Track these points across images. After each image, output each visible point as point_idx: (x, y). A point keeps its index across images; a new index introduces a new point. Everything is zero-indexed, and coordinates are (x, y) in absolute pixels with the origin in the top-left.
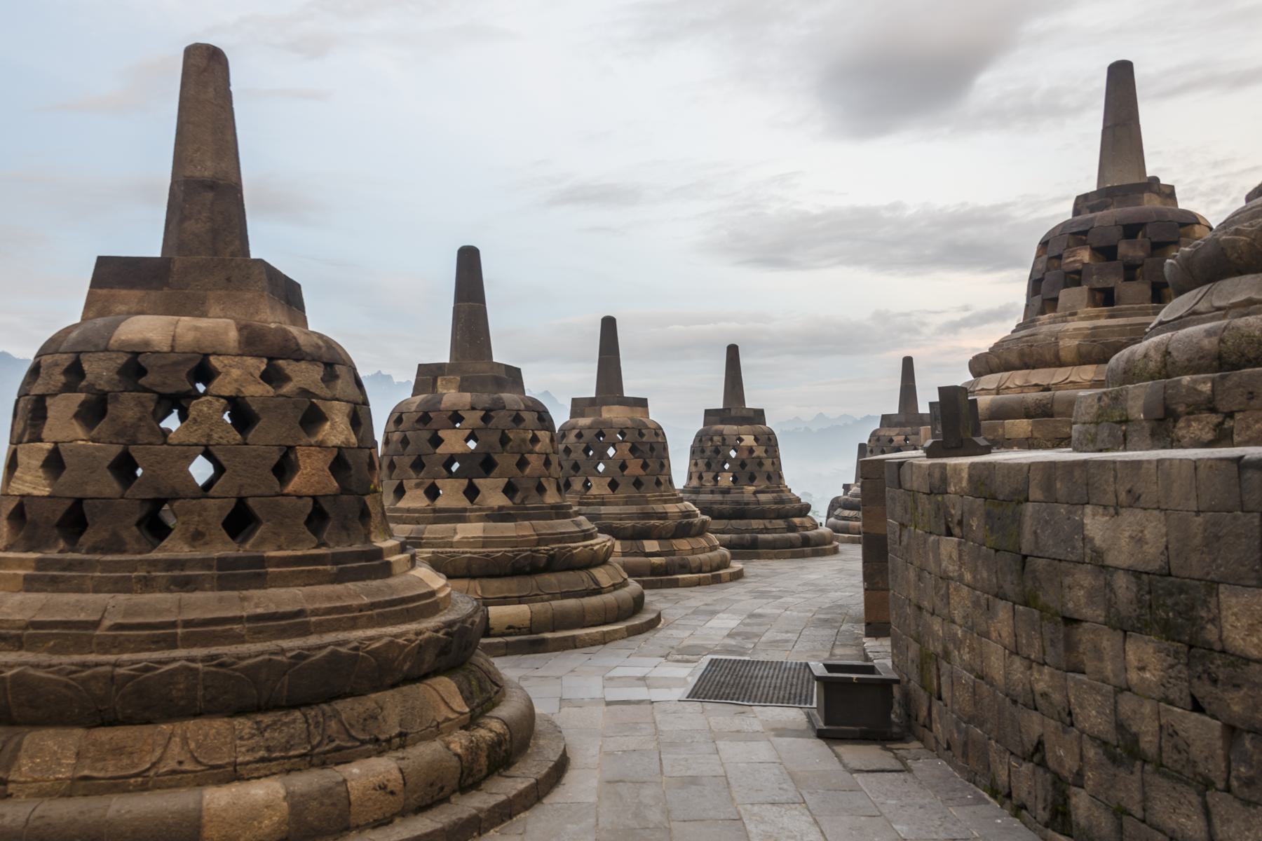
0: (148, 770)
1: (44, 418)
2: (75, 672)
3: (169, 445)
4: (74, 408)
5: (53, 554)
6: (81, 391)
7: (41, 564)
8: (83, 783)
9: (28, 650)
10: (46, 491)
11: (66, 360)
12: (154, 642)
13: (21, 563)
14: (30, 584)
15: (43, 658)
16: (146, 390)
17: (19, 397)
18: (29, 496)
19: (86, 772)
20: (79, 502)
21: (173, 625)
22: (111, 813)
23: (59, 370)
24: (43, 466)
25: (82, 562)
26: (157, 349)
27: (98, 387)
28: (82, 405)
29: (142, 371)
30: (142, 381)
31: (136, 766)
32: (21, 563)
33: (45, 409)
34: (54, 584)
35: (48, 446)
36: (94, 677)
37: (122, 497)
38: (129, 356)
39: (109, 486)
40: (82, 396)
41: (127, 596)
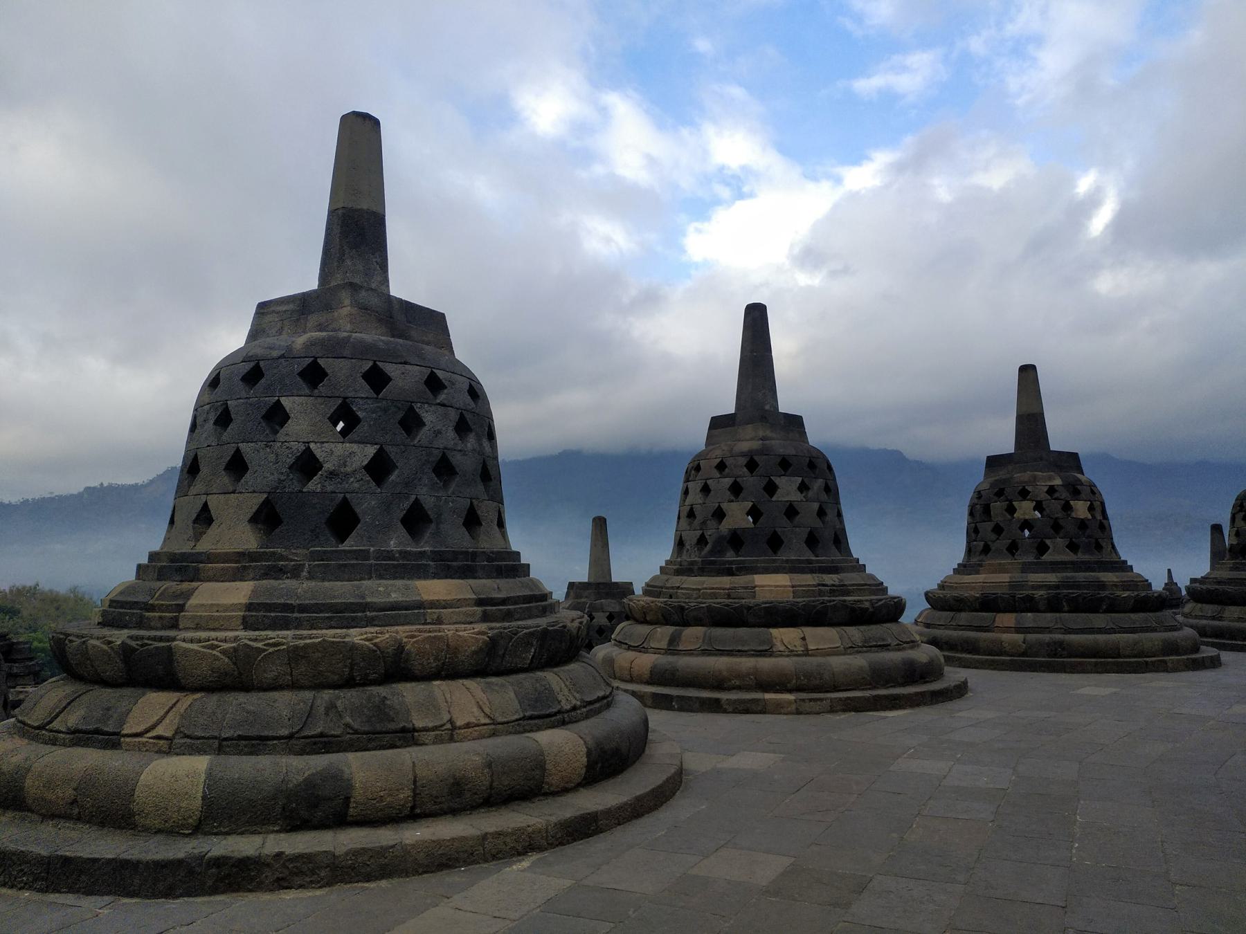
5: (1237, 561)
10: (1235, 543)
14: (1232, 569)
28: (1244, 516)
35: (1236, 529)
40: (1244, 513)
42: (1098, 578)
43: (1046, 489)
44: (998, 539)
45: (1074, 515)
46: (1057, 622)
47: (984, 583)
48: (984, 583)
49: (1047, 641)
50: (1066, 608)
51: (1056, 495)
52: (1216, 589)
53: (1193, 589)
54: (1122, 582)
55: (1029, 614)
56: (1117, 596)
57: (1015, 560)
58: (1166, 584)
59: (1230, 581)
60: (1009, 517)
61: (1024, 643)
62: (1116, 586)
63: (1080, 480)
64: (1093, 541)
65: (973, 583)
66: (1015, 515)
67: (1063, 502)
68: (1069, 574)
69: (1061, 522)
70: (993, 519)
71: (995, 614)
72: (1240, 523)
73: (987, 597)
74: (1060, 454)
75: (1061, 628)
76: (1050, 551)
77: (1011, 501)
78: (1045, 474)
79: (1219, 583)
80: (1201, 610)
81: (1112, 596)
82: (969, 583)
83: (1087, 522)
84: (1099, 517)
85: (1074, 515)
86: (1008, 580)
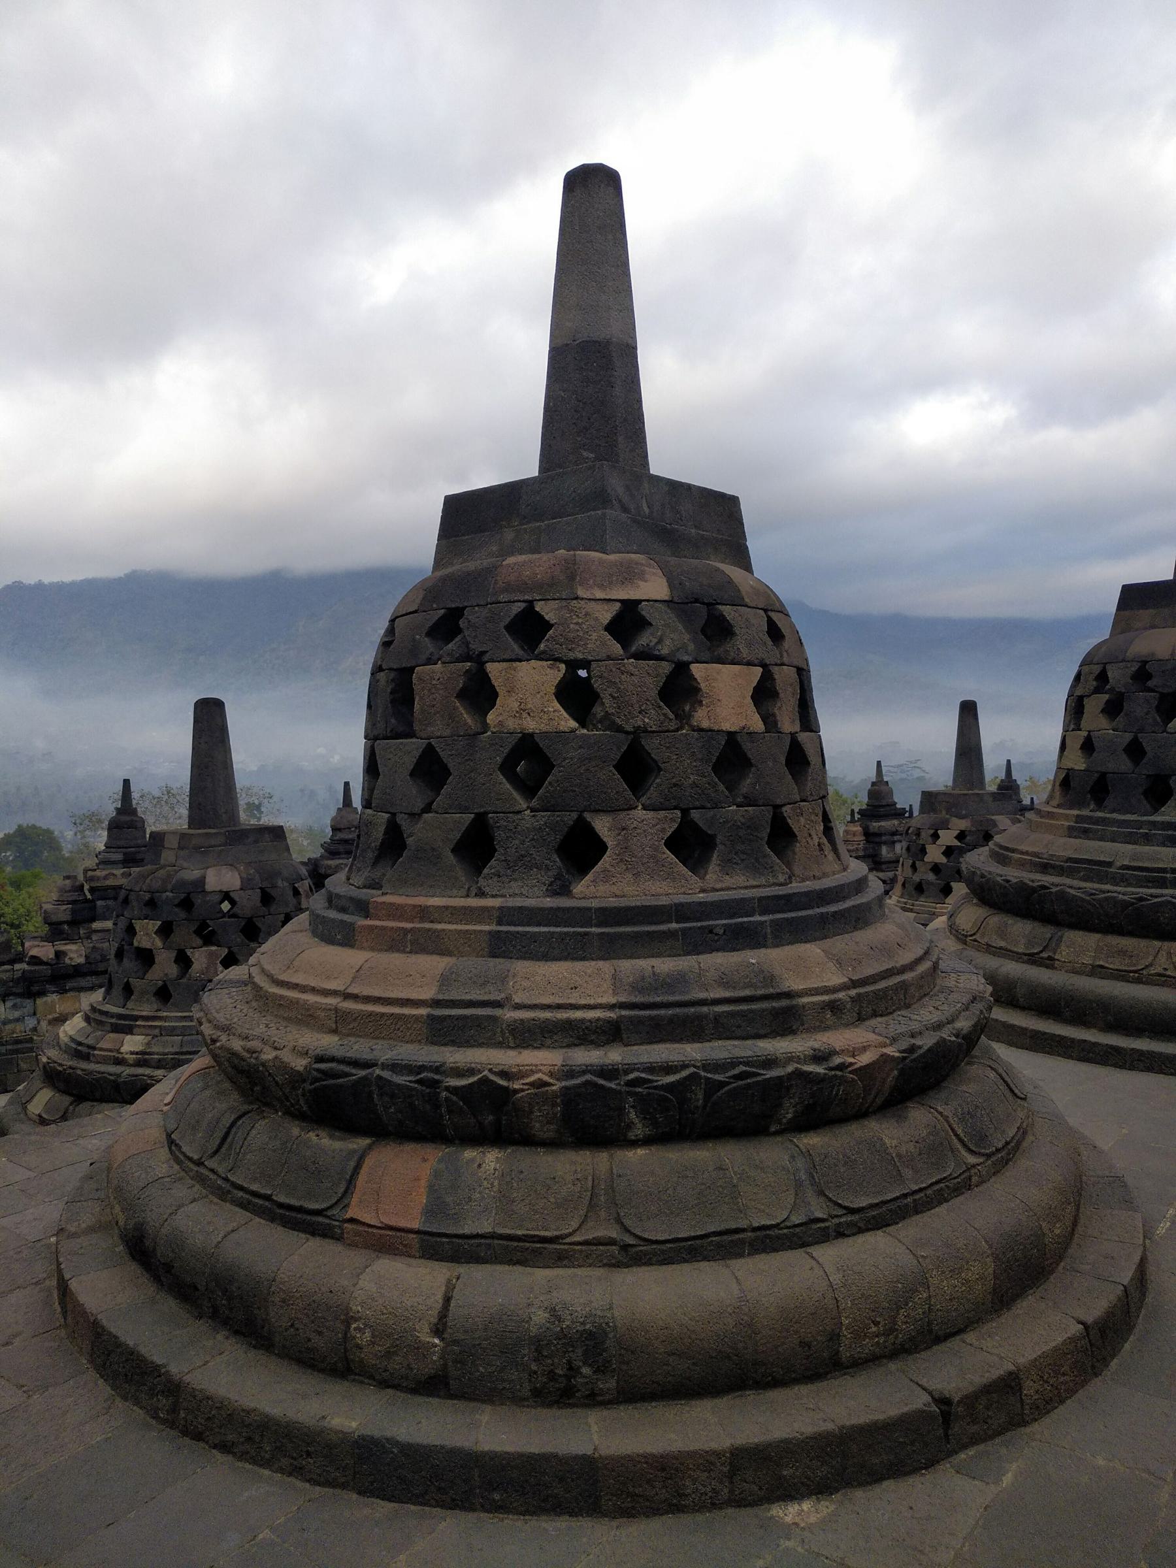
0: (1142, 969)
1: (1083, 713)
2: (1094, 894)
3: (1168, 733)
4: (1102, 706)
5: (1085, 812)
6: (1106, 693)
7: (1079, 819)
8: (1100, 970)
9: (1067, 877)
10: (1082, 767)
11: (1097, 669)
12: (1149, 881)
13: (1067, 817)
14: (1072, 832)
15: (1076, 883)
16: (1153, 691)
17: (1069, 696)
18: (1072, 769)
19: (1101, 963)
20: (1103, 775)
21: (1164, 870)
22: (1116, 992)
23: (1092, 677)
24: (1081, 748)
25: (1104, 819)
26: (1161, 658)
27: (1117, 690)
28: (1107, 702)
29: (1149, 676)
30: (1150, 684)
31: (1135, 965)
32: (1067, 817)
33: (1083, 706)
34: (1086, 833)
35: (1085, 734)
36: (1106, 899)
37: (1133, 773)
38: (1139, 664)
39: (1124, 764)
40: (1107, 696)
41: (1134, 846)
42: (771, 979)
43: (606, 614)
44: (428, 809)
45: (701, 718)
46: (592, 1206)
47: (347, 996)
48: (347, 996)
49: (534, 1331)
50: (639, 1130)
51: (644, 640)
52: (1044, 887)
53: (983, 876)
54: (854, 984)
55: (491, 1159)
56: (842, 1067)
57: (481, 894)
58: (873, 784)
59: (1071, 867)
60: (468, 718)
61: (438, 1331)
62: (834, 1007)
63: (730, 581)
64: (768, 813)
65: (313, 990)
66: (491, 717)
67: (666, 668)
68: (665, 965)
69: (652, 745)
70: (416, 727)
71: (364, 1142)
72: (1095, 720)
73: (327, 1074)
74: (676, 489)
75: (611, 1242)
76: (606, 861)
77: (479, 660)
78: (612, 557)
79: (1045, 868)
80: (1002, 933)
81: (819, 1069)
82: (303, 989)
83: (747, 746)
84: (788, 723)
85: (701, 718)
86: (428, 994)
